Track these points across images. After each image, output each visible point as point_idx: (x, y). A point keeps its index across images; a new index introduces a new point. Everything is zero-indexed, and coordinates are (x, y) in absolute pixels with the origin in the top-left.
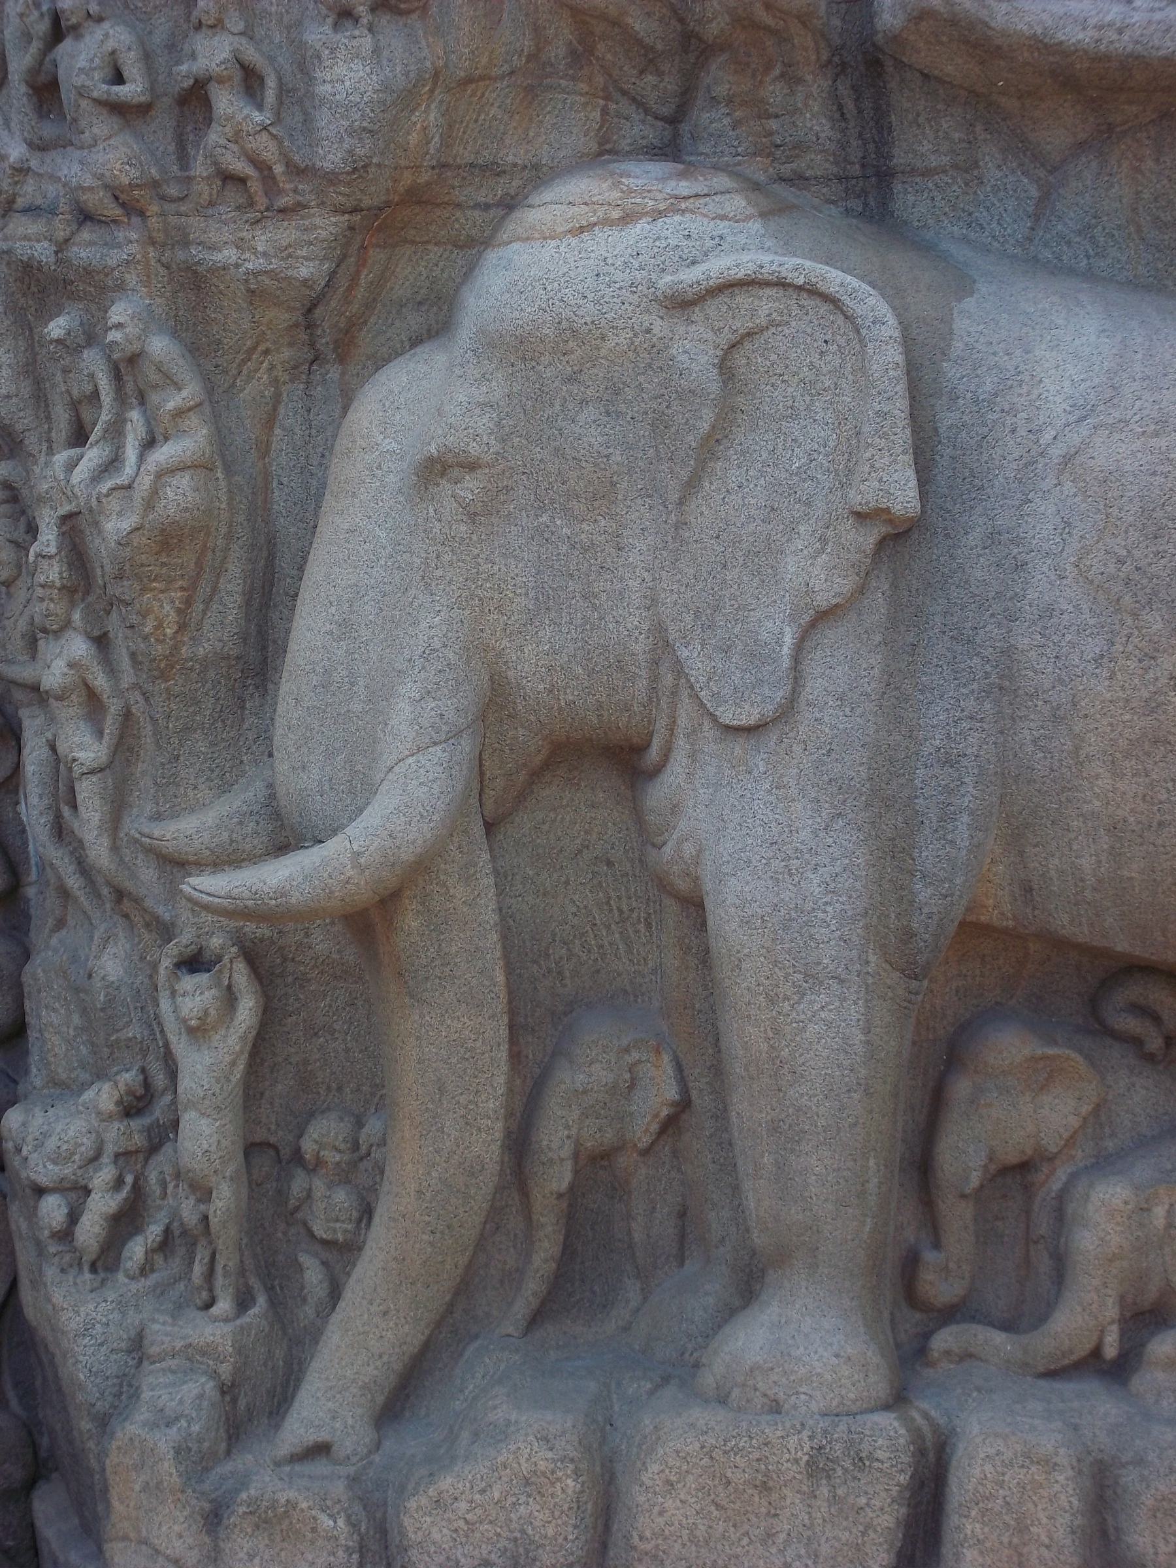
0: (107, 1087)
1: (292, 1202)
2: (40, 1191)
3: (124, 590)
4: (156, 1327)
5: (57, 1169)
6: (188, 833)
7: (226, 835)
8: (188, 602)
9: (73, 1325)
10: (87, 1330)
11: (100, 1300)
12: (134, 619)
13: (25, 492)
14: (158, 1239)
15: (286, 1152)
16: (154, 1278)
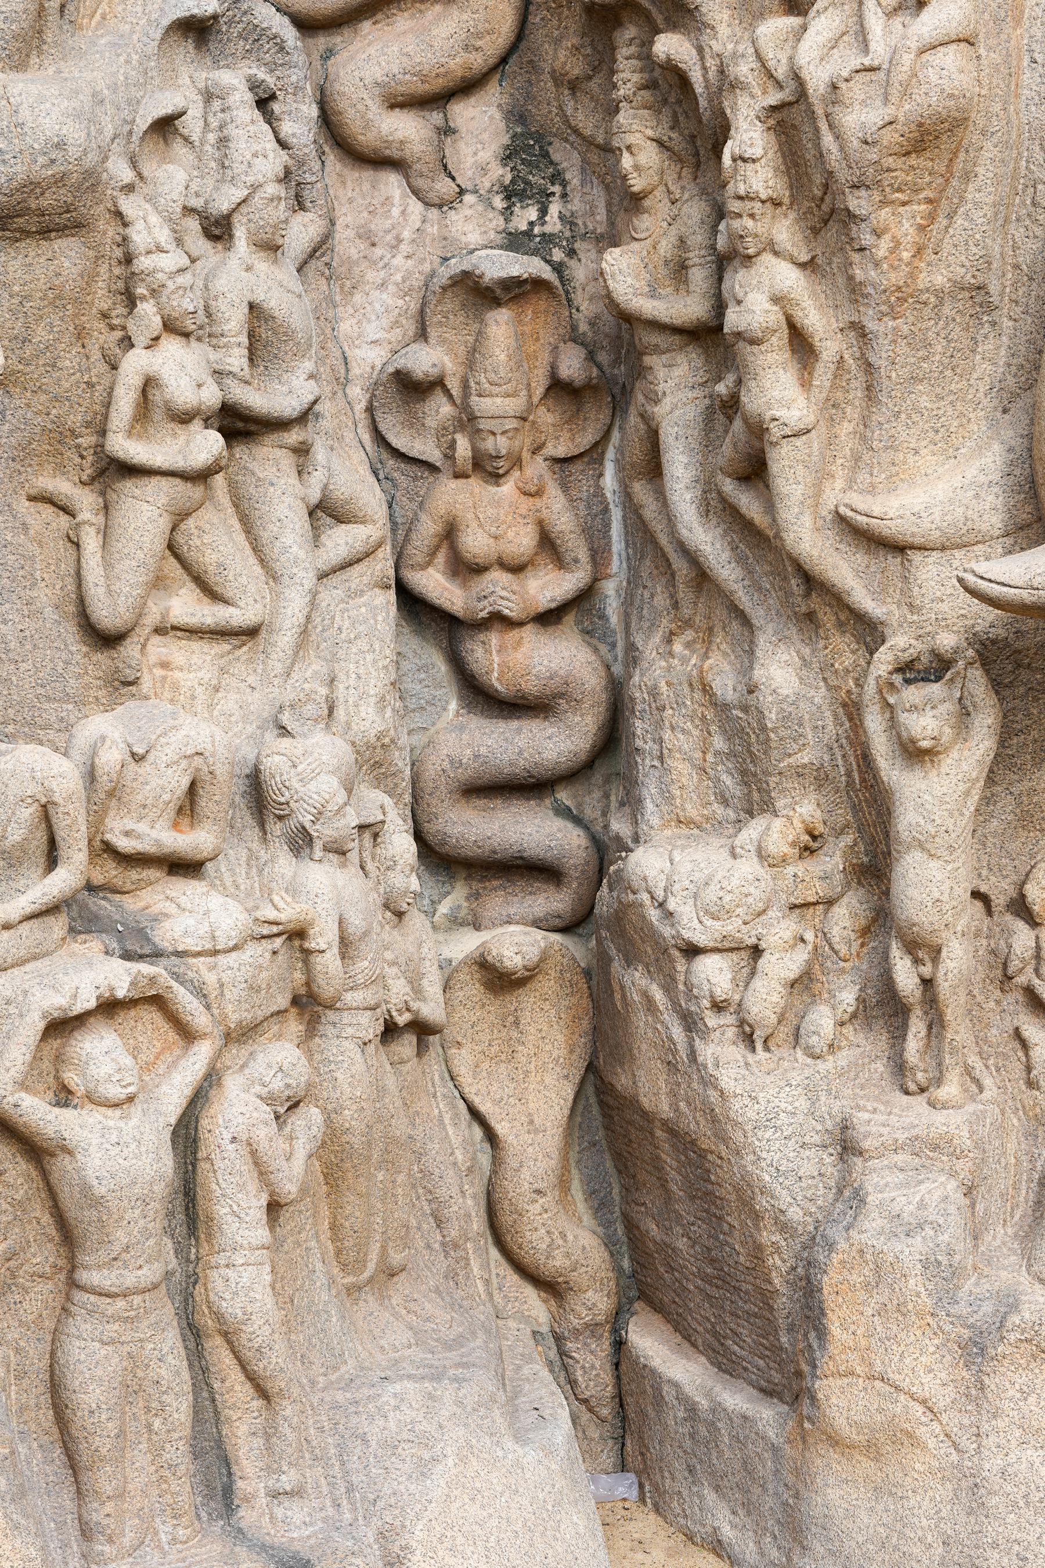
0: (778, 823)
1: (1014, 965)
2: (692, 951)
3: (858, 203)
4: (866, 1116)
5: (717, 924)
6: (915, 510)
7: (960, 510)
8: (932, 217)
9: (751, 1114)
10: (770, 1121)
11: (783, 1083)
12: (867, 239)
13: (696, 77)
14: (850, 1009)
15: (999, 901)
16: (843, 1058)
